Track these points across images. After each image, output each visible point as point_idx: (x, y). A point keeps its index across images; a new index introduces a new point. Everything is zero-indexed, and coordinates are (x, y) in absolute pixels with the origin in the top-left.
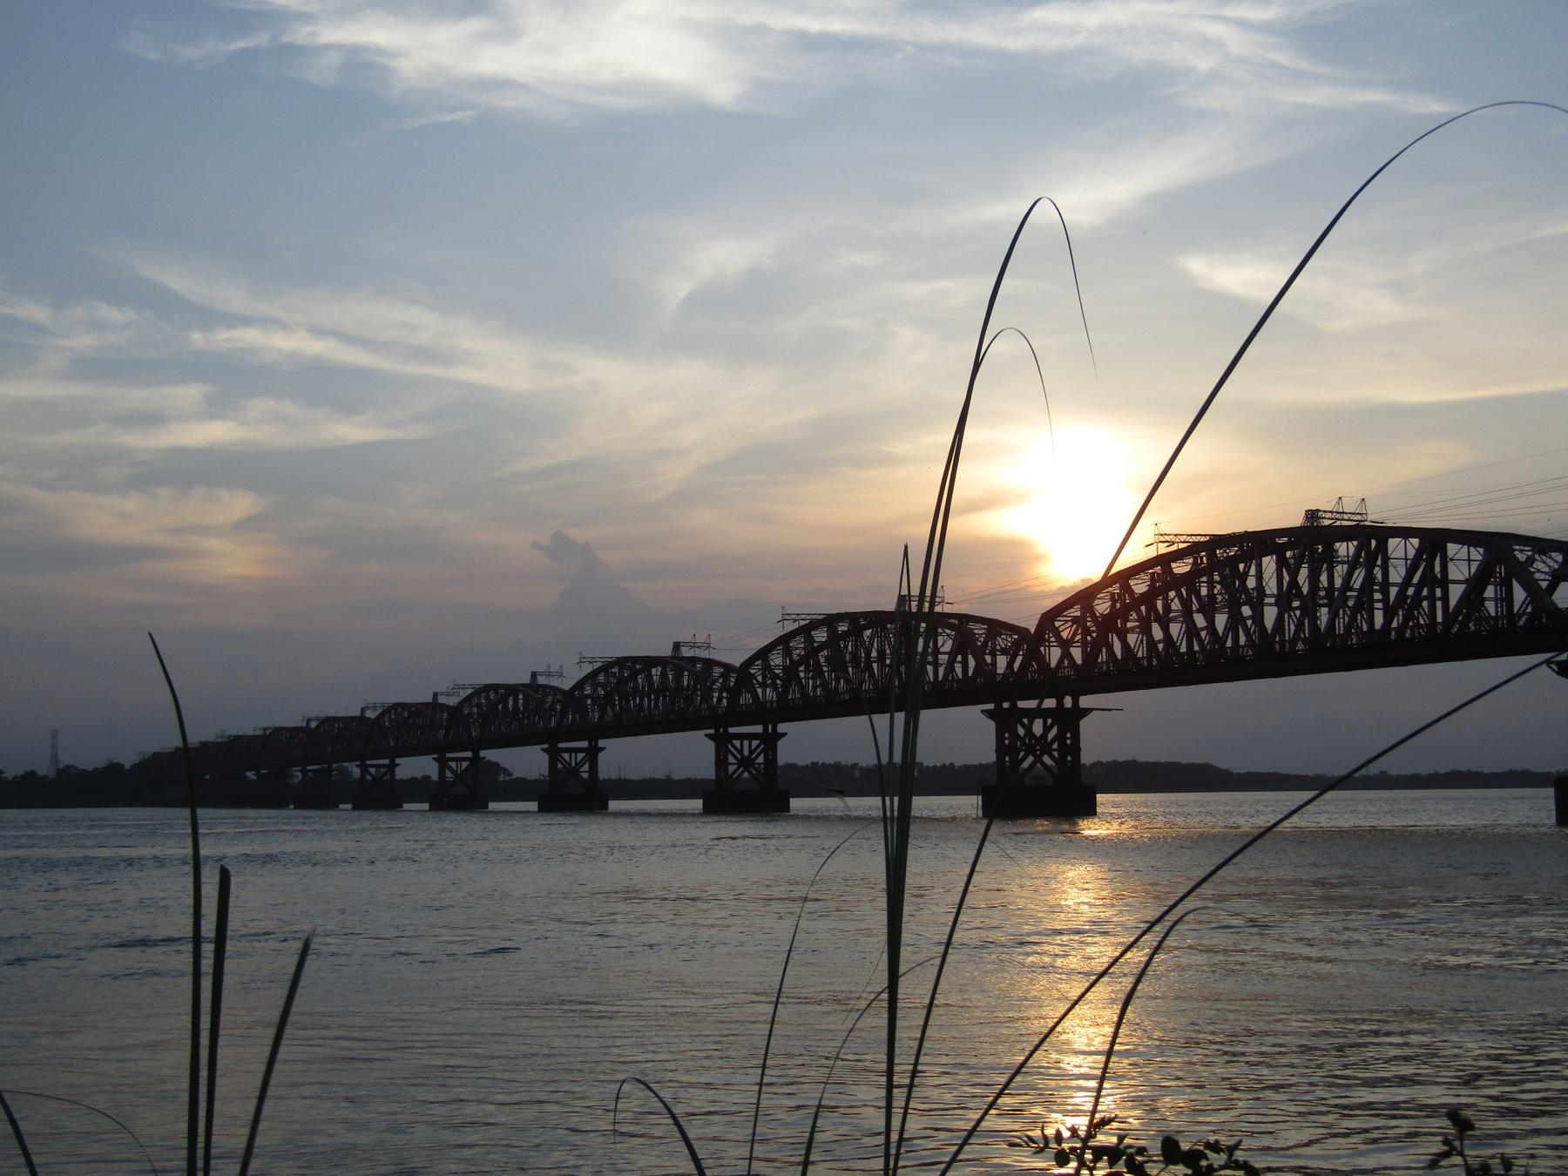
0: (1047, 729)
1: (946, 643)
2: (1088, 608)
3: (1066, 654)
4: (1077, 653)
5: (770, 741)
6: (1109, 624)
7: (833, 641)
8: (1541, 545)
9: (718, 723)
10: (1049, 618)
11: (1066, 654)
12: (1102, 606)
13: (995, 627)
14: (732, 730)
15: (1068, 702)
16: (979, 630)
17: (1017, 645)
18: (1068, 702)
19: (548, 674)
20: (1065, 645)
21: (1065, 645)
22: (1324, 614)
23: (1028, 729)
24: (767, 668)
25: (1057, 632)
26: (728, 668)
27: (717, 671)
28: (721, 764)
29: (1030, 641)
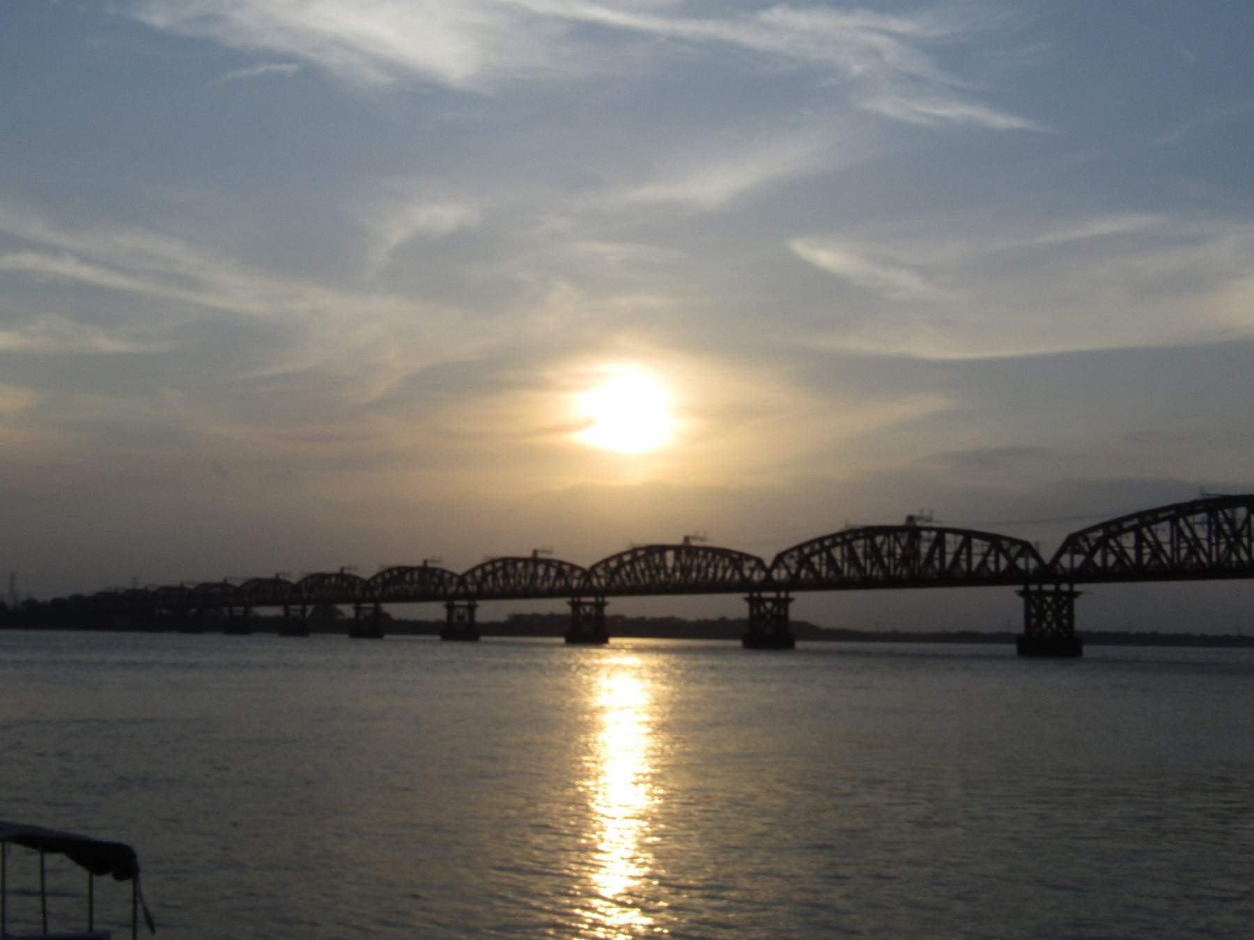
1: (553, 572)
3: (599, 583)
5: (472, 609)
6: (617, 571)
7: (504, 567)
8: (749, 557)
9: (448, 598)
10: (593, 568)
11: (599, 583)
12: (613, 564)
13: (573, 567)
16: (566, 568)
20: (599, 577)
21: (599, 577)
23: (584, 609)
25: (596, 573)
29: (588, 574)
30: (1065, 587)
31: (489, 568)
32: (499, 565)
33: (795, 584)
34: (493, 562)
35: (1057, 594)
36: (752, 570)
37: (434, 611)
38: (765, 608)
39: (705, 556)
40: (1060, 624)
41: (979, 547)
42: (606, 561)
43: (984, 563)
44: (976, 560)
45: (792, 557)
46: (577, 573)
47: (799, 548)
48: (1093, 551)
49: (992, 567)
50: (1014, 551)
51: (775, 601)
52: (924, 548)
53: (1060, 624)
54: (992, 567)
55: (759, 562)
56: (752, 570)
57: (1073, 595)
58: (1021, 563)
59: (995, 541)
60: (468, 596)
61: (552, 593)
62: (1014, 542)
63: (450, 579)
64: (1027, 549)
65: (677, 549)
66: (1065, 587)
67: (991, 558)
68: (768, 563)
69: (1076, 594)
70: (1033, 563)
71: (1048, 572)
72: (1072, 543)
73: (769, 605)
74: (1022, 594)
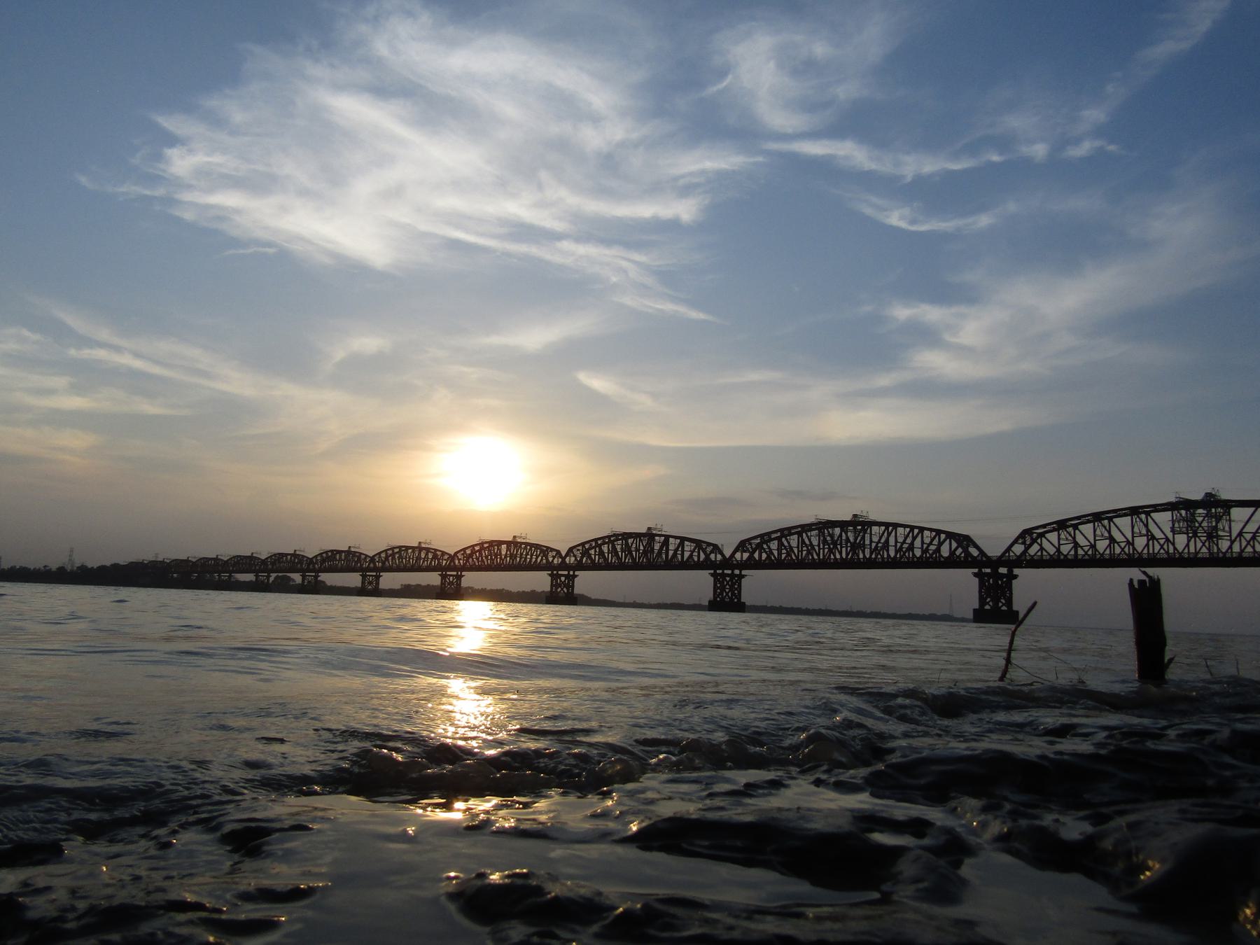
0: (454, 579)
1: (430, 556)
2: (465, 552)
3: (459, 562)
4: (461, 562)
6: (471, 556)
7: (399, 552)
8: (552, 550)
10: (456, 553)
11: (459, 562)
12: (468, 552)
13: (444, 553)
14: (367, 573)
15: (459, 573)
16: (439, 553)
17: (448, 558)
18: (459, 573)
19: (300, 551)
20: (459, 560)
21: (459, 560)
22: (518, 559)
23: (449, 579)
24: (380, 557)
26: (366, 556)
27: (363, 557)
28: (363, 583)
29: (452, 557)
30: (737, 572)
31: (390, 552)
32: (396, 550)
33: (580, 566)
34: (393, 549)
35: (732, 576)
36: (554, 557)
37: (354, 579)
38: (561, 581)
39: (525, 548)
40: (733, 594)
41: (688, 547)
42: (464, 550)
43: (691, 556)
44: (687, 555)
45: (578, 550)
46: (446, 557)
47: (583, 544)
48: (754, 551)
49: (696, 559)
50: (709, 549)
51: (567, 576)
52: (657, 547)
53: (733, 594)
54: (696, 559)
55: (558, 552)
56: (554, 557)
57: (741, 577)
58: (712, 556)
59: (698, 544)
60: (375, 569)
61: (429, 569)
62: (709, 544)
63: (365, 558)
64: (716, 549)
65: (508, 543)
66: (737, 572)
67: (695, 554)
68: (564, 554)
69: (744, 576)
70: (719, 557)
71: (727, 563)
72: (742, 546)
73: (563, 579)
74: (712, 575)
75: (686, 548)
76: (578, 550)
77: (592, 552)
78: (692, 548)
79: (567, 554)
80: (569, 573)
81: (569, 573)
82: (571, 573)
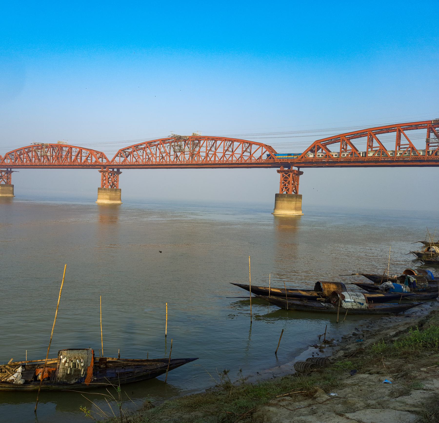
44: (84, 159)
45: (13, 155)
48: (127, 157)
50: (98, 155)
52: (64, 153)
54: (89, 161)
62: (98, 152)
64: (102, 155)
70: (105, 161)
72: (119, 154)
73: (3, 173)
75: (83, 155)
76: (13, 155)
77: (22, 156)
78: (87, 154)
79: (5, 158)
80: (7, 170)
81: (7, 170)
82: (9, 169)
